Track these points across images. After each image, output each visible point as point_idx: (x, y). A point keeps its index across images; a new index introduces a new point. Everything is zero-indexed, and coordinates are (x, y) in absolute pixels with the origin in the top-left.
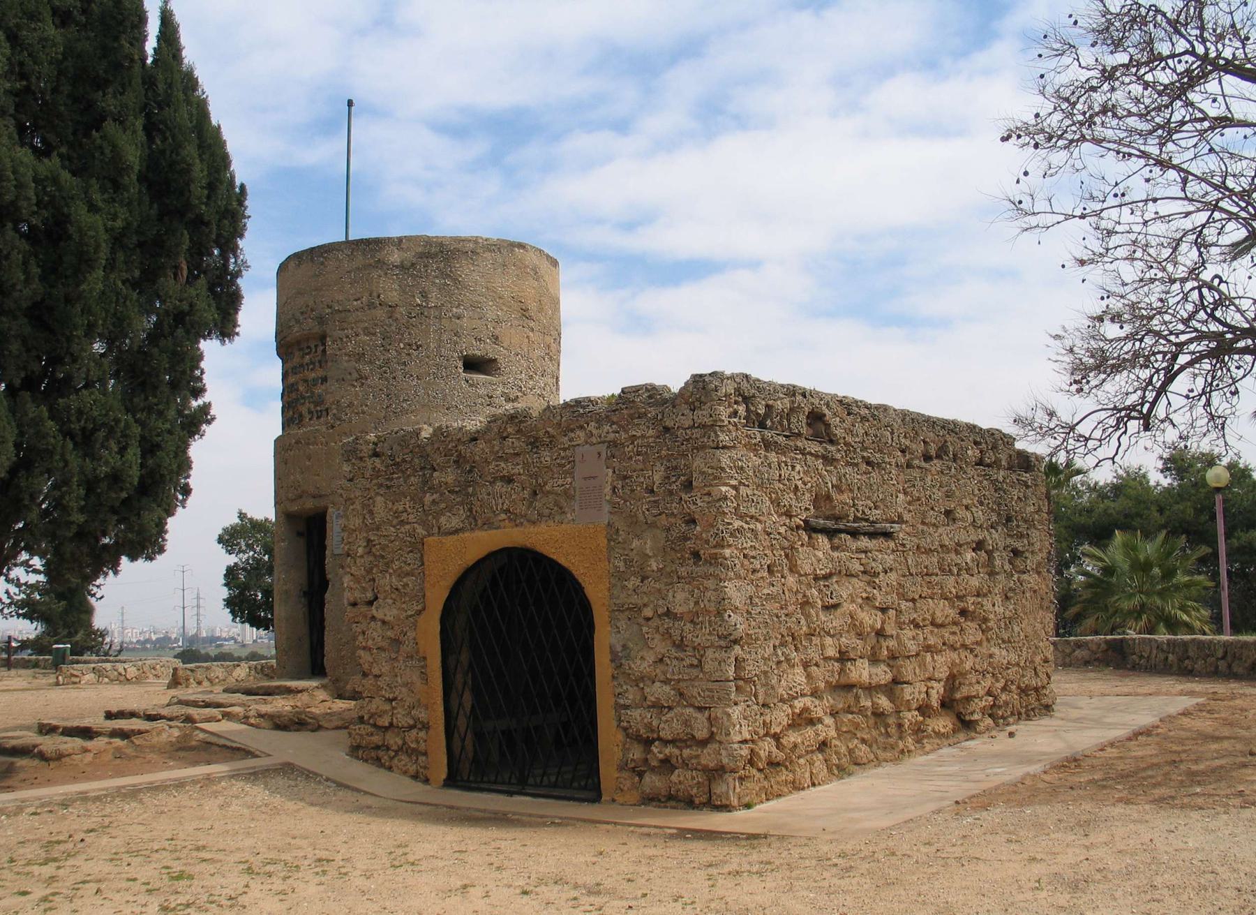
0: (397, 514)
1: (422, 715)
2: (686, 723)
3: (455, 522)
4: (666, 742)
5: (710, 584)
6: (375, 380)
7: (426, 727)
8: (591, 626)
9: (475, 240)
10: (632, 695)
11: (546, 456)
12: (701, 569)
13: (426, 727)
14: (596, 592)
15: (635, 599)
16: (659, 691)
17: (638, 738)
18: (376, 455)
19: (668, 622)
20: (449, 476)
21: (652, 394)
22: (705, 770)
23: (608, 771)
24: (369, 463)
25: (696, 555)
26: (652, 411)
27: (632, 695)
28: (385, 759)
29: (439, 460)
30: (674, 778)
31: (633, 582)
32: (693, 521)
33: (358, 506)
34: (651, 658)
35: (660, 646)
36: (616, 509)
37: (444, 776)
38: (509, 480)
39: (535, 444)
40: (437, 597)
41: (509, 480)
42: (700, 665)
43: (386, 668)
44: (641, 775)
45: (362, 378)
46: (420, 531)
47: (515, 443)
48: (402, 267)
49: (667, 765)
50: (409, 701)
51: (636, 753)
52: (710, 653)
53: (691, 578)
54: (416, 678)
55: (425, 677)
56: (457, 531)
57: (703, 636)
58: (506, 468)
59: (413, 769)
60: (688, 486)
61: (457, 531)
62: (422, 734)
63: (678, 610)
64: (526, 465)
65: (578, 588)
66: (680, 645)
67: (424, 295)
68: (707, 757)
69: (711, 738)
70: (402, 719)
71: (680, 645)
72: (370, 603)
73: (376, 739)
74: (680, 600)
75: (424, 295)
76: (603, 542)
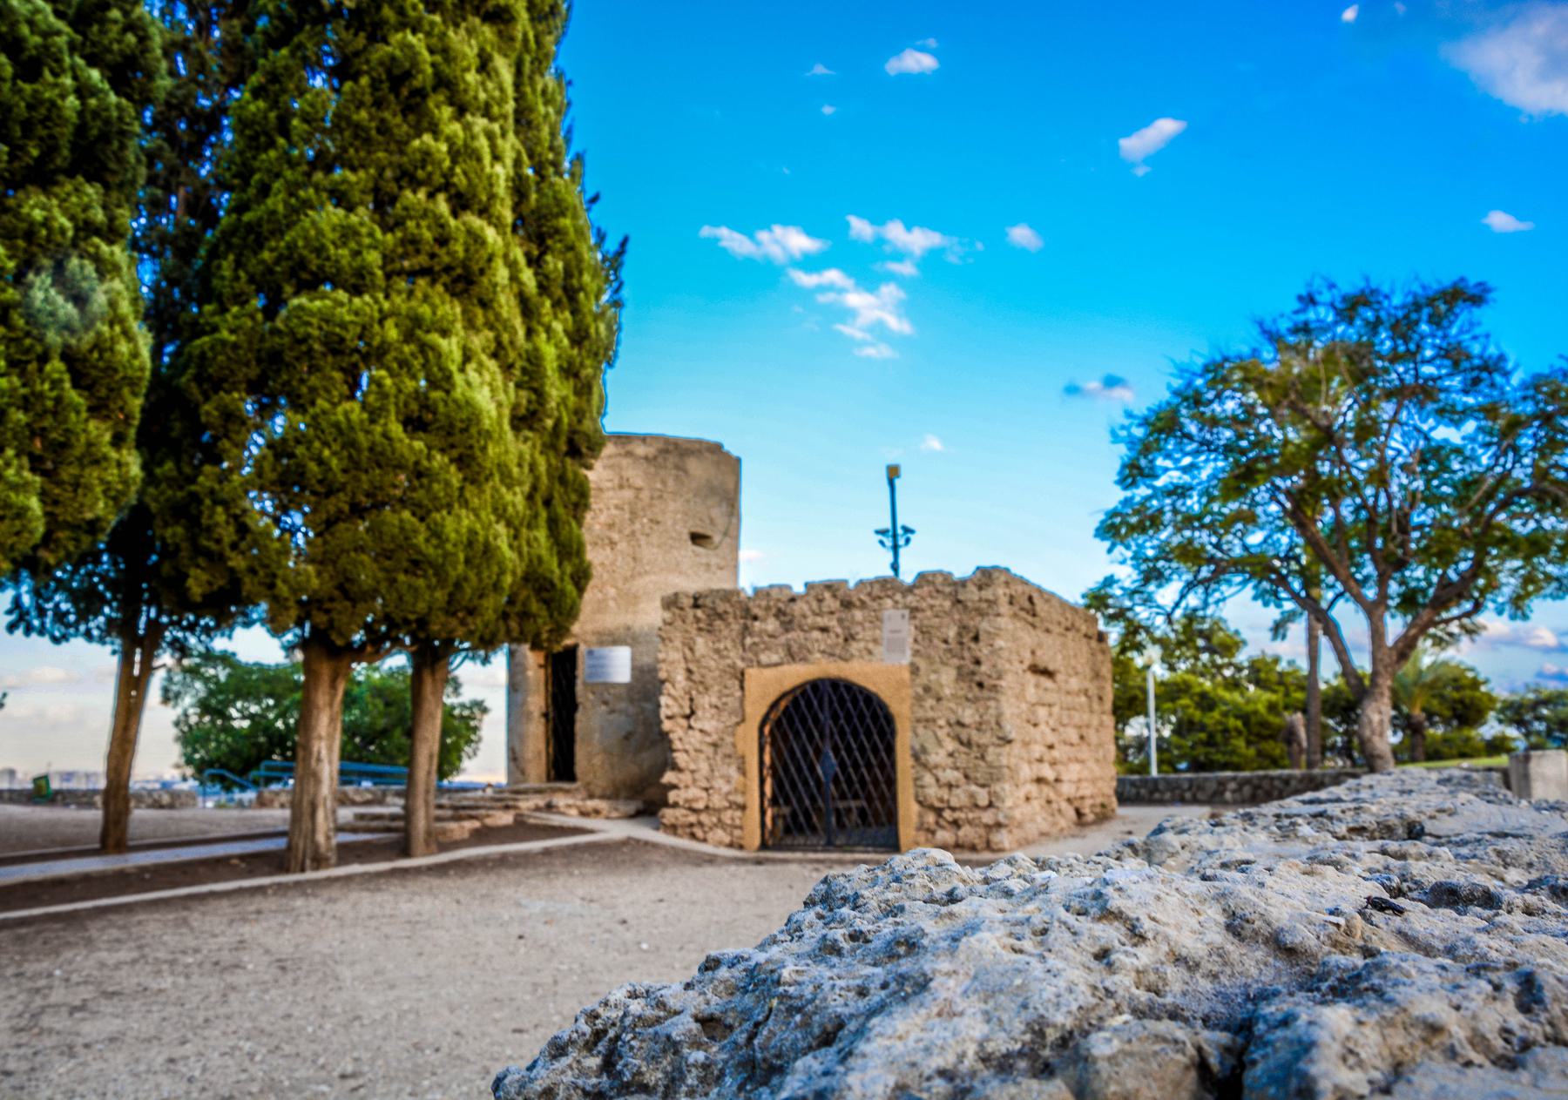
0: (717, 651)
1: (739, 799)
2: (972, 796)
3: (775, 658)
4: (953, 809)
5: (992, 704)
6: (622, 546)
7: (743, 808)
8: (893, 733)
9: (700, 442)
10: (928, 779)
11: (858, 615)
12: (985, 693)
13: (743, 808)
14: (901, 708)
15: (930, 714)
16: (950, 775)
17: (932, 808)
18: (696, 606)
19: (958, 729)
20: (772, 625)
21: (947, 577)
22: (988, 827)
23: (907, 831)
24: (690, 613)
25: (980, 685)
26: (947, 590)
27: (928, 779)
28: (699, 833)
29: (756, 611)
30: (961, 833)
31: (930, 702)
32: (978, 662)
33: (678, 643)
34: (942, 753)
35: (951, 745)
36: (916, 653)
37: (757, 841)
38: (824, 630)
39: (847, 605)
40: (756, 710)
41: (824, 630)
42: (983, 758)
43: (704, 767)
44: (933, 833)
45: (612, 544)
46: (740, 664)
47: (831, 603)
48: (646, 458)
49: (956, 824)
50: (726, 788)
51: (931, 818)
52: (991, 750)
53: (976, 700)
54: (733, 772)
55: (743, 771)
56: (776, 665)
57: (985, 739)
58: (821, 621)
59: (727, 839)
60: (976, 639)
61: (776, 665)
62: (738, 813)
63: (967, 721)
64: (840, 621)
65: (883, 706)
66: (968, 744)
67: (664, 483)
68: (988, 817)
69: (991, 805)
70: (717, 801)
71: (968, 744)
72: (688, 717)
73: (693, 818)
74: (968, 715)
75: (664, 483)
76: (906, 675)
